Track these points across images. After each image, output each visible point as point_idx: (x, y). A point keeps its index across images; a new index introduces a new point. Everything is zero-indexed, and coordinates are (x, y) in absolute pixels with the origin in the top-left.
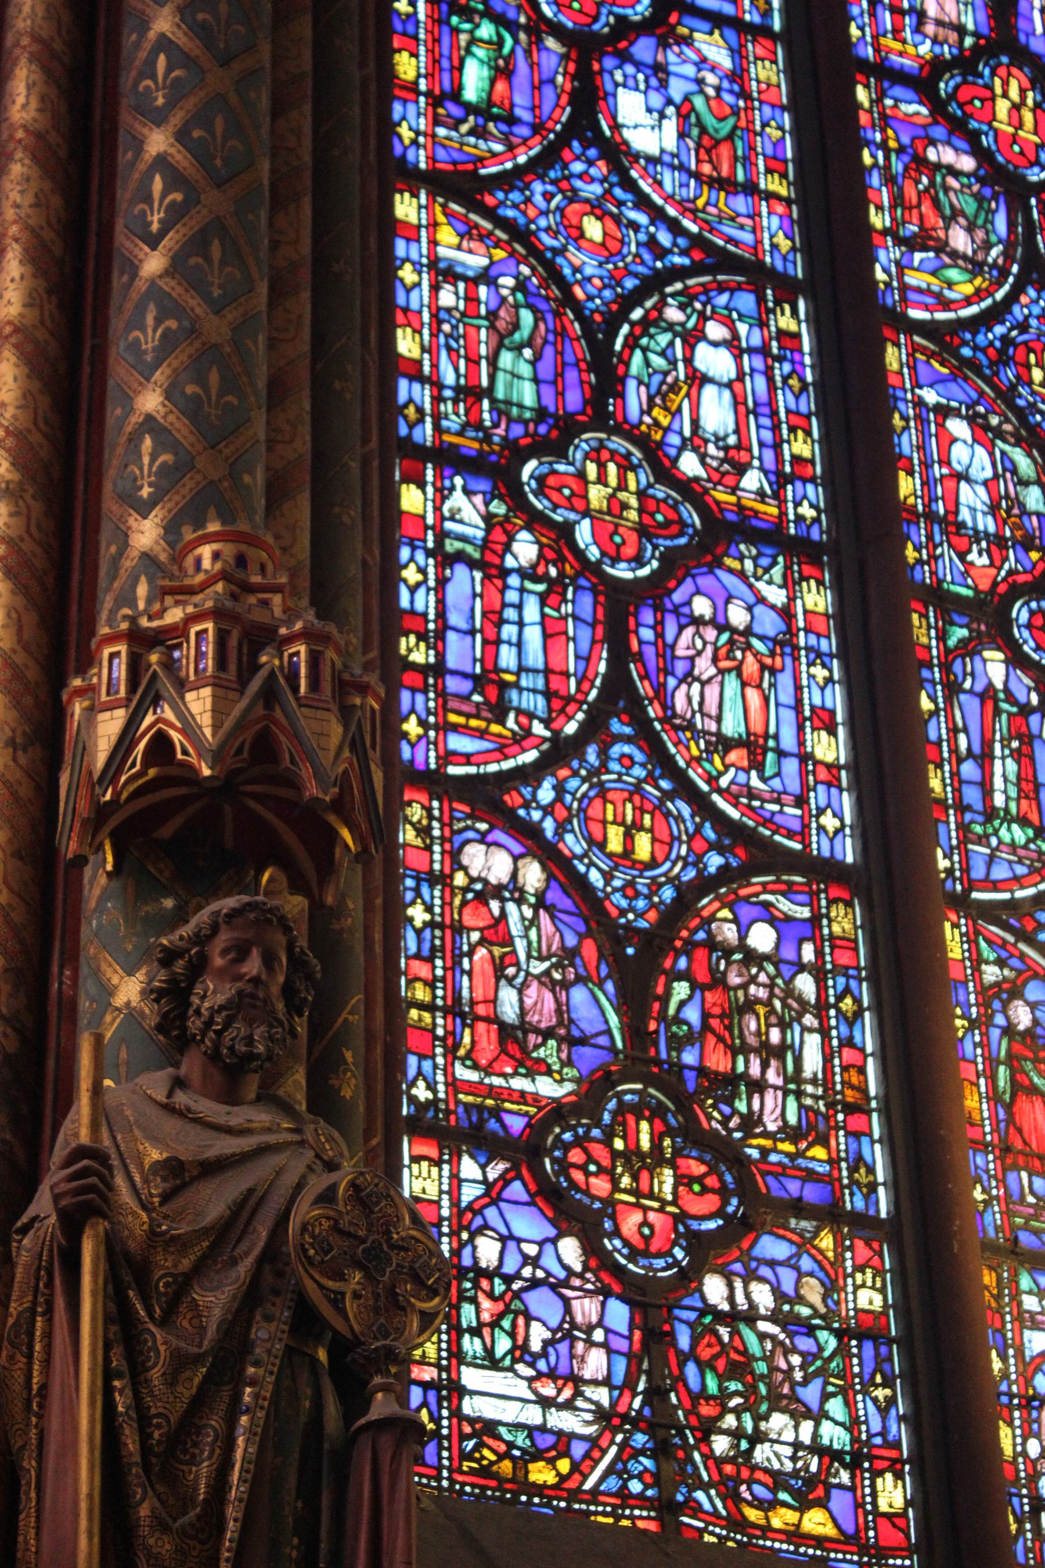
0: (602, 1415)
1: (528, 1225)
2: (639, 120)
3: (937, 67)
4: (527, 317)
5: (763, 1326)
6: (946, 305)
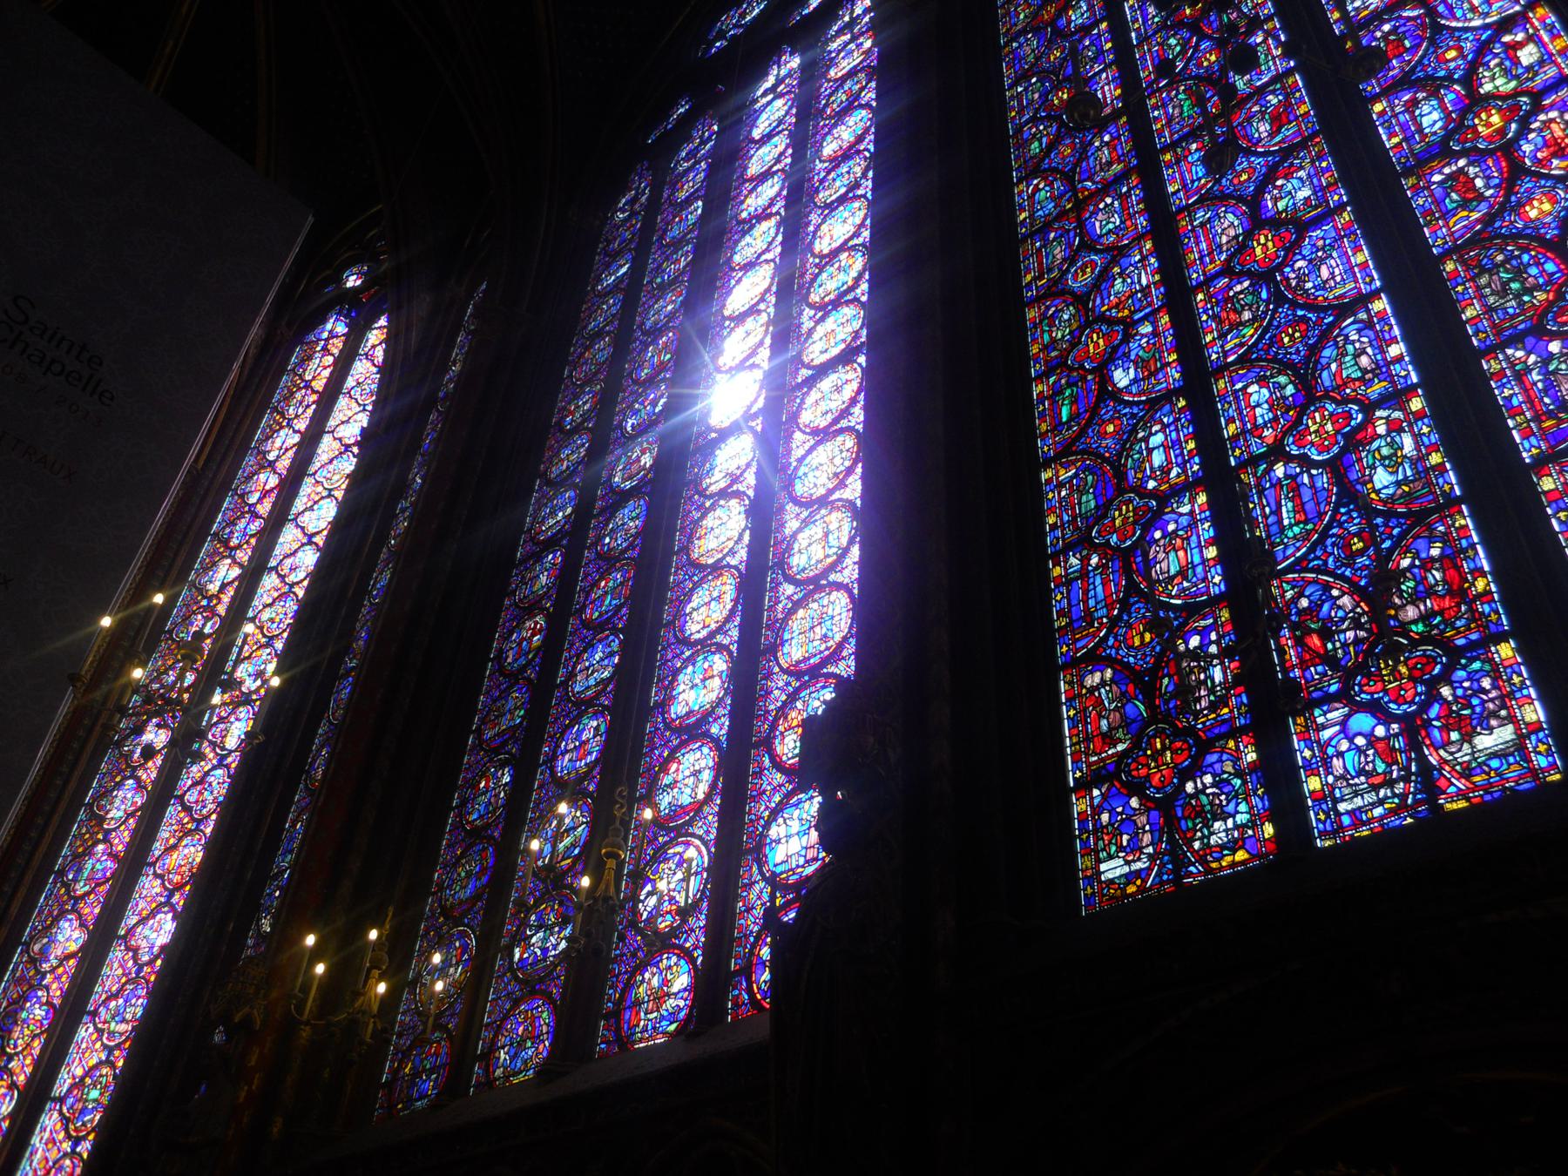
0: (1151, 857)
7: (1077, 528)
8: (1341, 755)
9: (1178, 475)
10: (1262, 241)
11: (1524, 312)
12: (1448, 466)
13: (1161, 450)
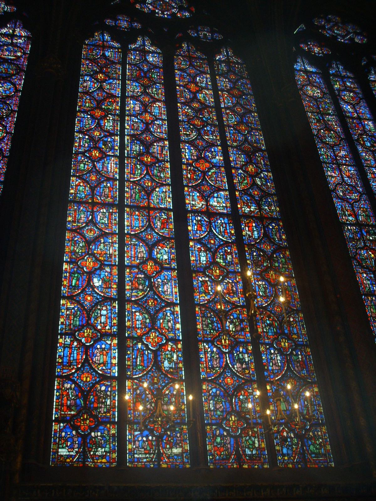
0: (76, 452)
2: (97, 282)
3: (139, 264)
4: (79, 313)
5: (99, 438)
8: (139, 441)
9: (109, 329)
10: (151, 265)
11: (210, 335)
12: (183, 369)
13: (105, 317)
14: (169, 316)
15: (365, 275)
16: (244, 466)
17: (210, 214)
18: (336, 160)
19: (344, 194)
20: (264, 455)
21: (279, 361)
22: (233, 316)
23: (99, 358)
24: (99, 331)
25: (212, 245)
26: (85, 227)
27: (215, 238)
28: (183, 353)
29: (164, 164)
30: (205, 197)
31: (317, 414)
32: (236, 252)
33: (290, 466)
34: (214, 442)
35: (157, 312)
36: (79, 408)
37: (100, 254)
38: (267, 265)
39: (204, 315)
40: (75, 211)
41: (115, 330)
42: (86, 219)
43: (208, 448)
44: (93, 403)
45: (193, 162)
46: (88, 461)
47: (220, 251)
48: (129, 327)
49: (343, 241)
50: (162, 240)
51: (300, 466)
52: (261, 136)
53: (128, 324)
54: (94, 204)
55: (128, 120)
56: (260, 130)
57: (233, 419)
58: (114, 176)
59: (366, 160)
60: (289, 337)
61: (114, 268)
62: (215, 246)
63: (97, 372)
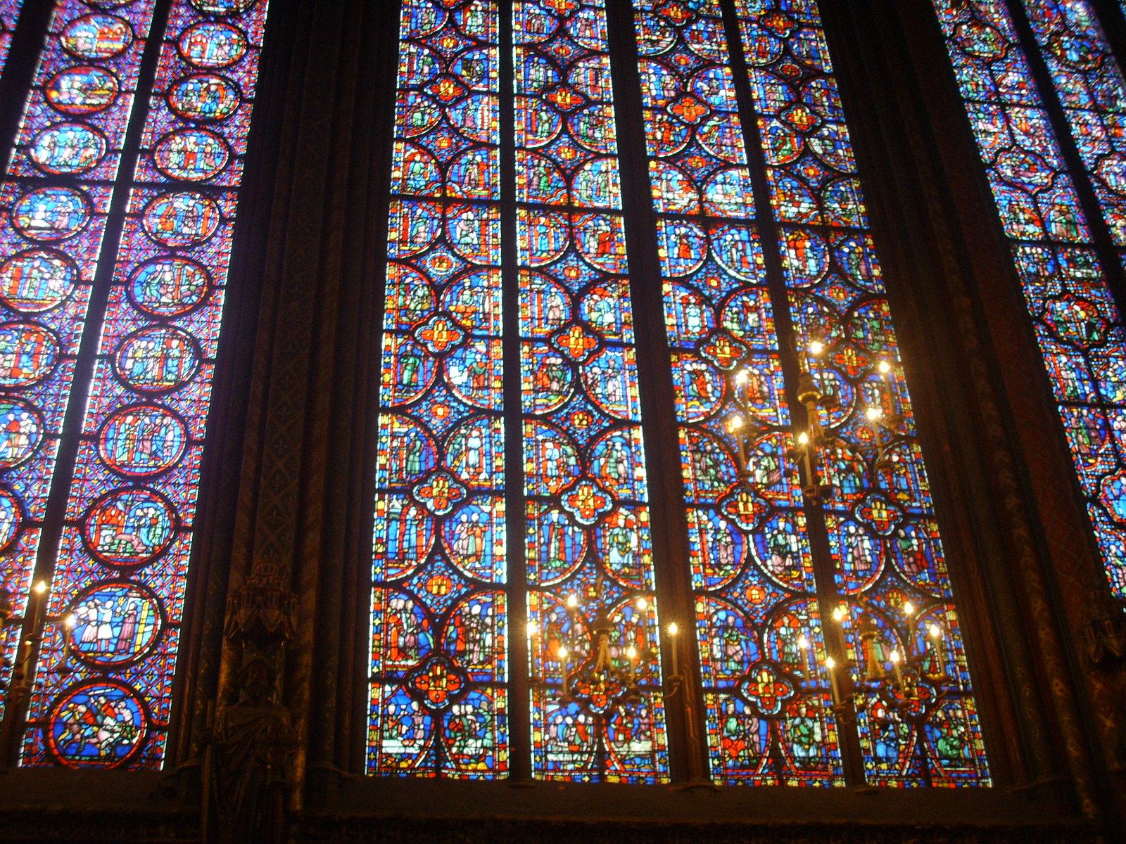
0: (420, 747)
1: (403, 702)
2: (456, 375)
3: (552, 334)
4: (418, 443)
6: (547, 407)
7: (401, 480)
8: (556, 725)
9: (485, 480)
10: (577, 335)
12: (652, 568)
14: (620, 452)
15: (1064, 359)
16: (789, 783)
17: (708, 221)
18: (998, 93)
19: (1017, 174)
20: (834, 758)
21: (867, 552)
22: (762, 450)
23: (465, 543)
24: (465, 484)
25: (714, 292)
26: (427, 253)
27: (720, 276)
28: (652, 531)
29: (601, 110)
30: (696, 184)
31: (954, 670)
32: (769, 305)
33: (893, 784)
34: (722, 729)
35: (593, 440)
36: (423, 652)
37: (463, 313)
38: (839, 336)
39: (699, 448)
40: (405, 217)
41: (499, 481)
42: (430, 236)
43: (710, 741)
44: (455, 641)
45: (667, 104)
46: (446, 768)
47: (732, 304)
48: (531, 476)
49: (1014, 282)
50: (602, 280)
51: (914, 785)
52: (822, 41)
53: (528, 467)
54: (447, 202)
55: (517, 12)
56: (819, 29)
57: (766, 680)
58: (489, 138)
59: (1069, 94)
60: (889, 498)
61: (494, 343)
62: (721, 292)
63: (461, 575)
